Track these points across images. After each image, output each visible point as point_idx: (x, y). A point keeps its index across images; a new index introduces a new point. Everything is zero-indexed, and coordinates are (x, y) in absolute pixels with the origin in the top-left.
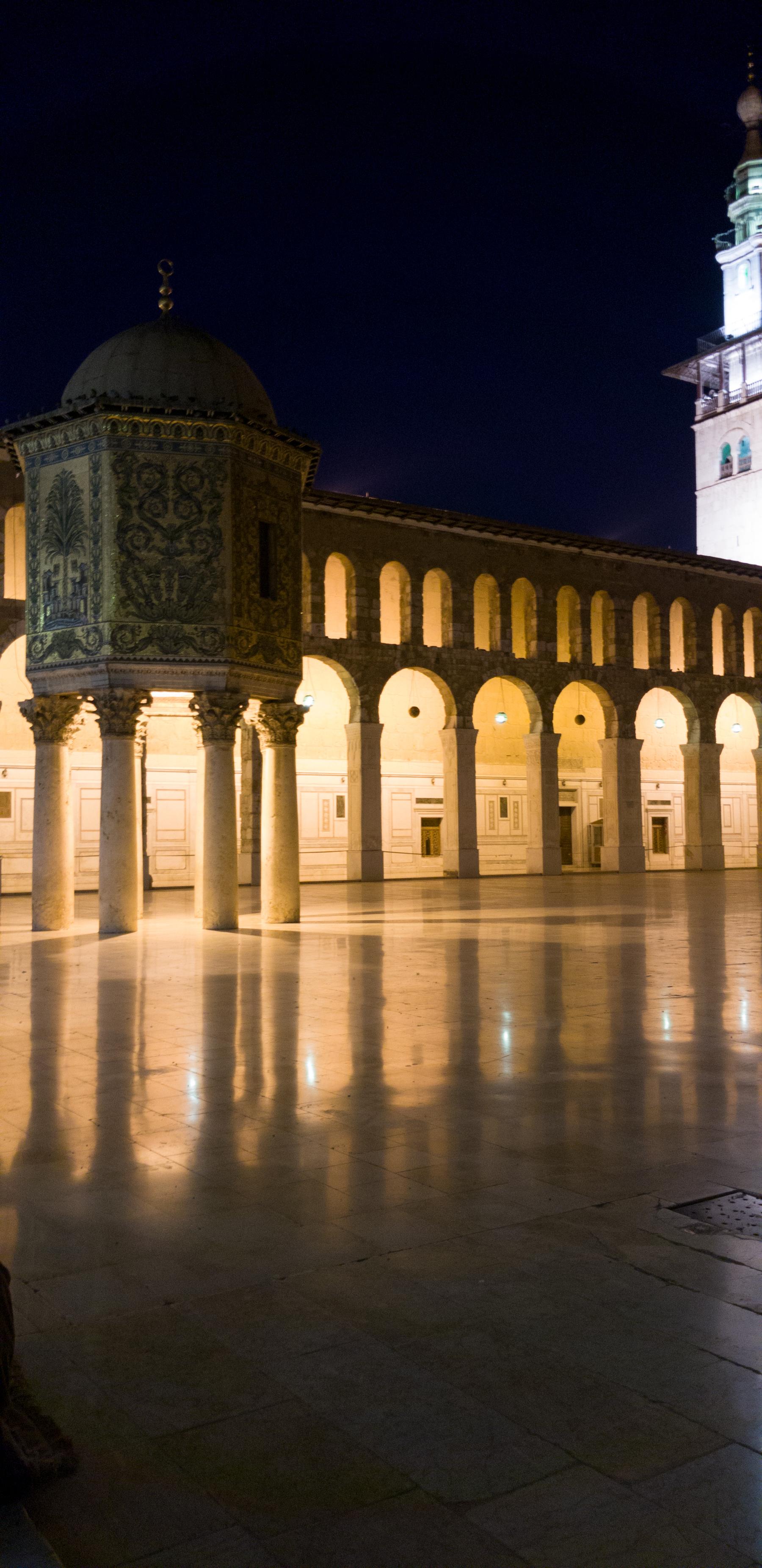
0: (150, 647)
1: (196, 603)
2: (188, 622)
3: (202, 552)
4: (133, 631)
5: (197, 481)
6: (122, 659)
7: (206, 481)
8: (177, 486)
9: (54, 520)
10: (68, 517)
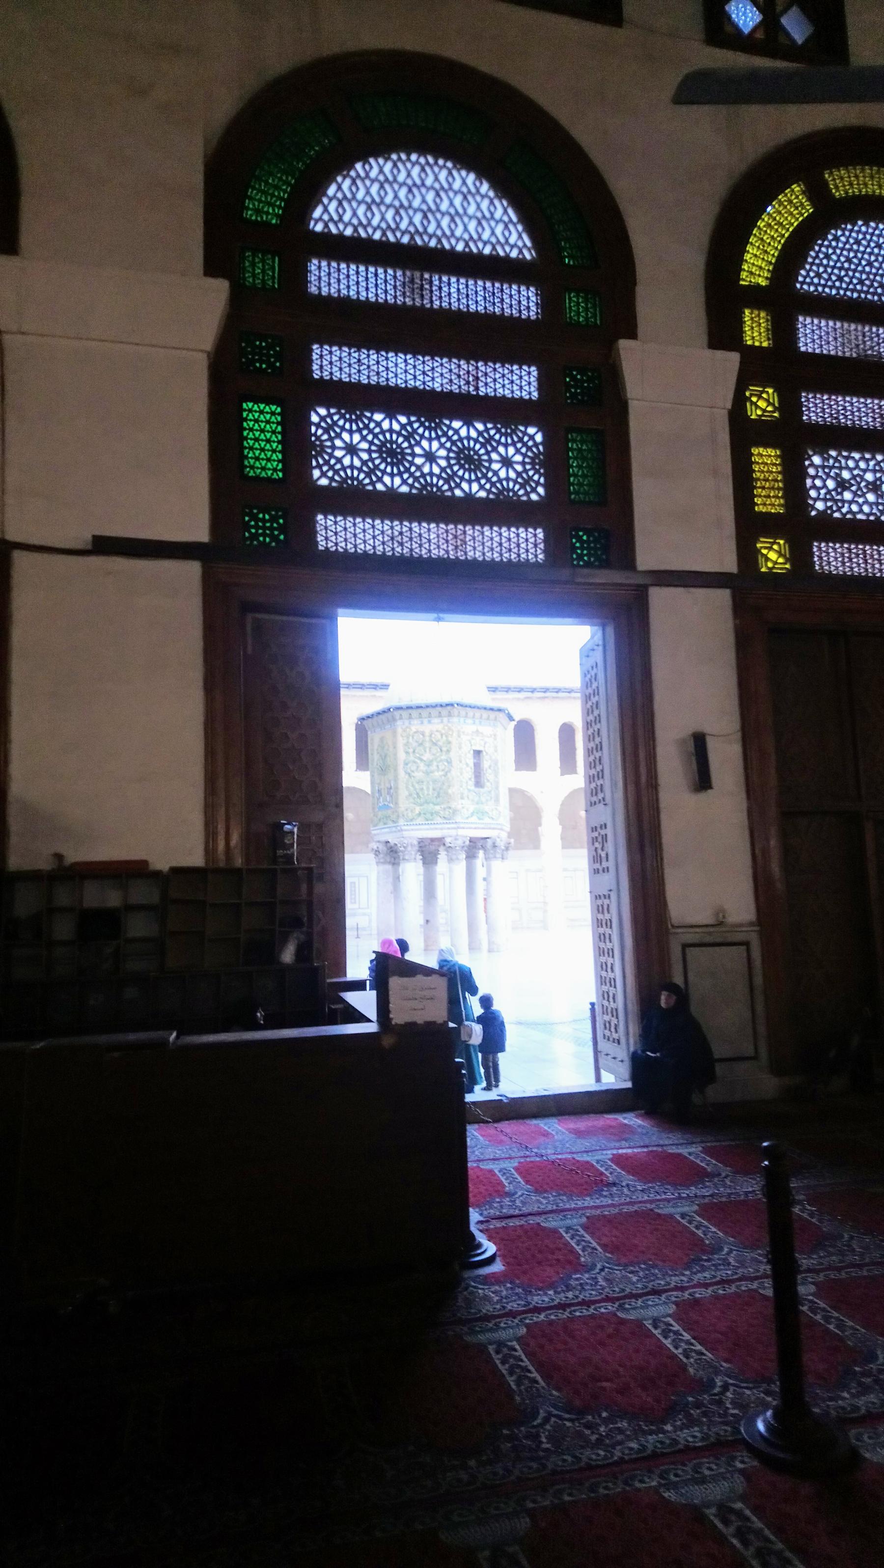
2: (437, 804)
4: (412, 811)
5: (439, 736)
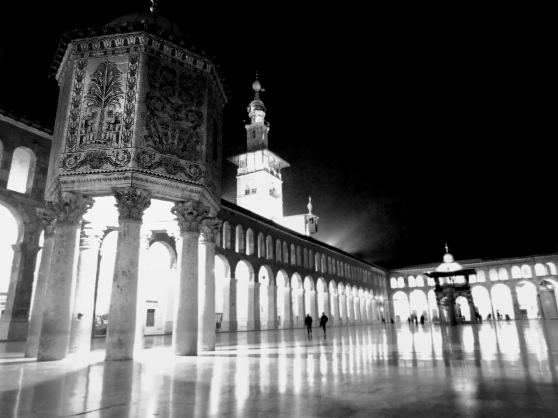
0: (160, 168)
1: (187, 149)
3: (192, 122)
4: (150, 156)
6: (142, 172)
9: (96, 87)
10: (107, 87)
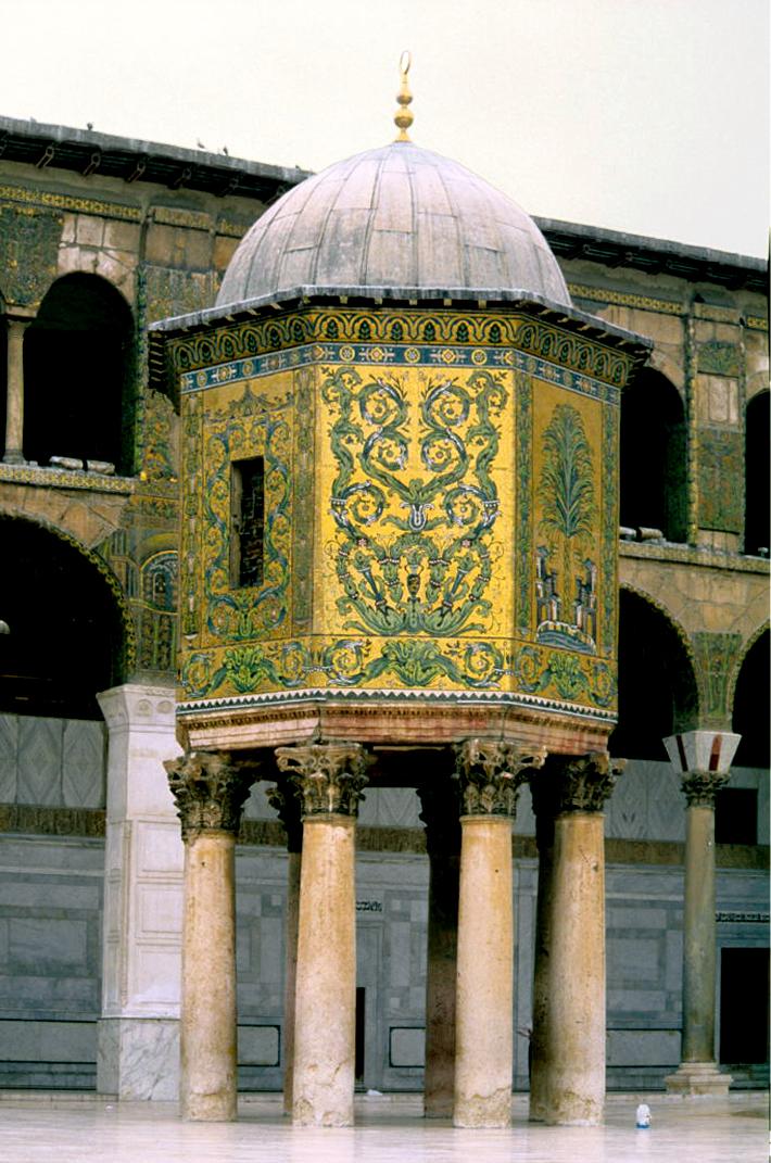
4: (358, 651)
5: (458, 409)
7: (473, 407)
8: (428, 419)
